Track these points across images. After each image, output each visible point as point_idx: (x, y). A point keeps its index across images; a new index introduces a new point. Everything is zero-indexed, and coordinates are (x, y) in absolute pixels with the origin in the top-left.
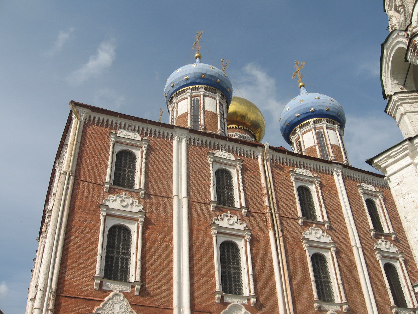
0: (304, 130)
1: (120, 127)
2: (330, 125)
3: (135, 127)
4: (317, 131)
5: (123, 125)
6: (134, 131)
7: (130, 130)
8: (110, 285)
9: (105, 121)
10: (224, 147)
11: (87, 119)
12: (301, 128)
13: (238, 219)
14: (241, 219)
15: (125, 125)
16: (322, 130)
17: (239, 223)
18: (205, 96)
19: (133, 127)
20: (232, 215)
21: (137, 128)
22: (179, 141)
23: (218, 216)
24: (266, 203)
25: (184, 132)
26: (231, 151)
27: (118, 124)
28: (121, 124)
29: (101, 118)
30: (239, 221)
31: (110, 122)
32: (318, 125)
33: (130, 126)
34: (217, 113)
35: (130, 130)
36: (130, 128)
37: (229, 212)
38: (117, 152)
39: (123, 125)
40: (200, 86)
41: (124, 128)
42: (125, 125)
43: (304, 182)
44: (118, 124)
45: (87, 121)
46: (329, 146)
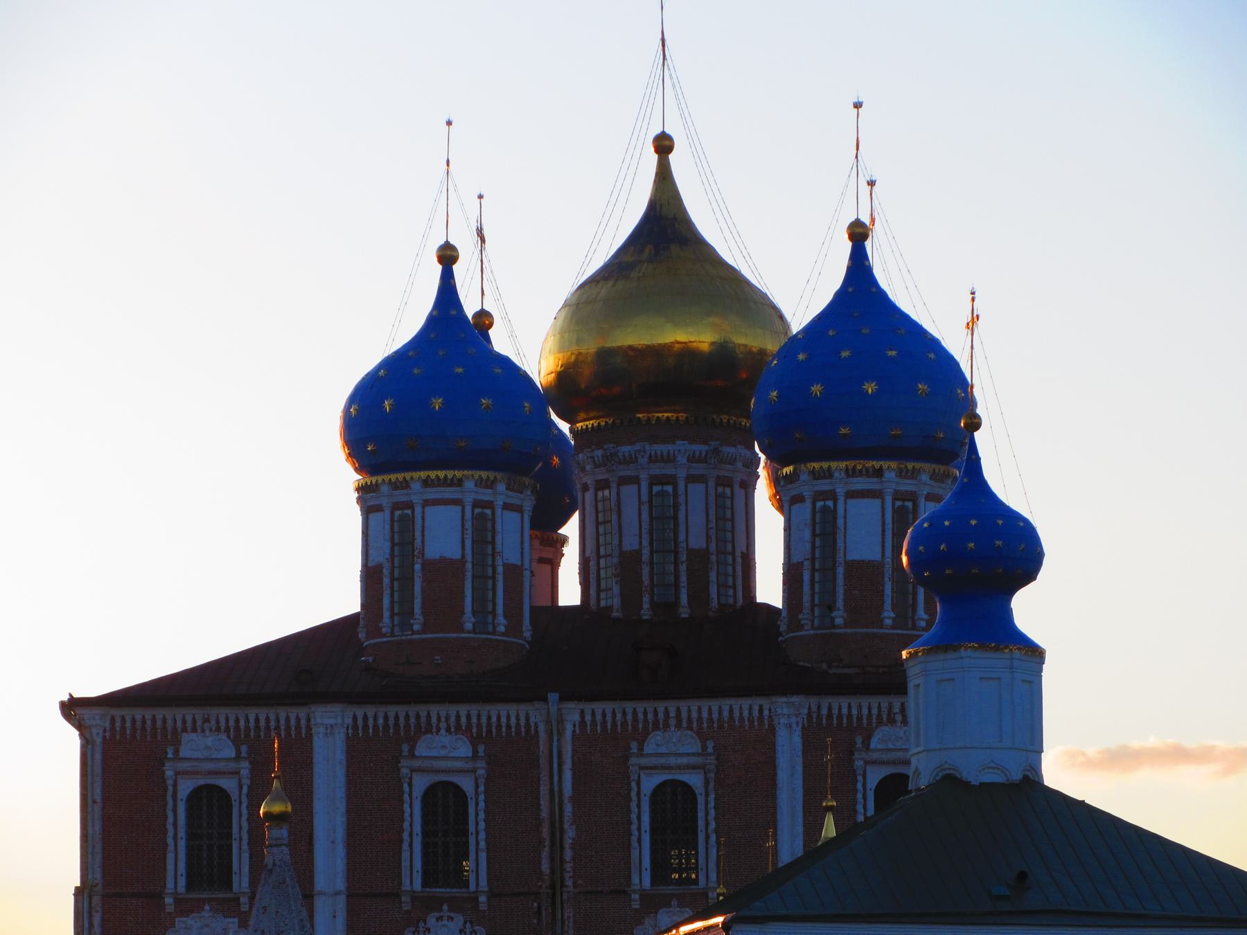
1: (185, 730)
2: (860, 484)
3: (218, 722)
4: (820, 504)
5: (189, 724)
6: (218, 729)
7: (207, 732)
9: (149, 723)
10: (443, 719)
11: (108, 729)
13: (465, 922)
15: (194, 721)
16: (830, 503)
17: (468, 931)
18: (427, 503)
19: (213, 723)
20: (452, 915)
21: (223, 724)
23: (418, 921)
24: (545, 867)
25: (333, 709)
26: (464, 728)
27: (179, 724)
28: (184, 722)
29: (138, 717)
30: (468, 925)
31: (159, 724)
32: (824, 485)
33: (207, 720)
34: (463, 556)
35: (207, 732)
36: (206, 725)
37: (445, 907)
38: (184, 799)
39: (189, 724)
40: (408, 475)
41: (194, 730)
42: (194, 721)
43: (674, 771)
44: (179, 724)
45: (108, 734)
46: (840, 571)
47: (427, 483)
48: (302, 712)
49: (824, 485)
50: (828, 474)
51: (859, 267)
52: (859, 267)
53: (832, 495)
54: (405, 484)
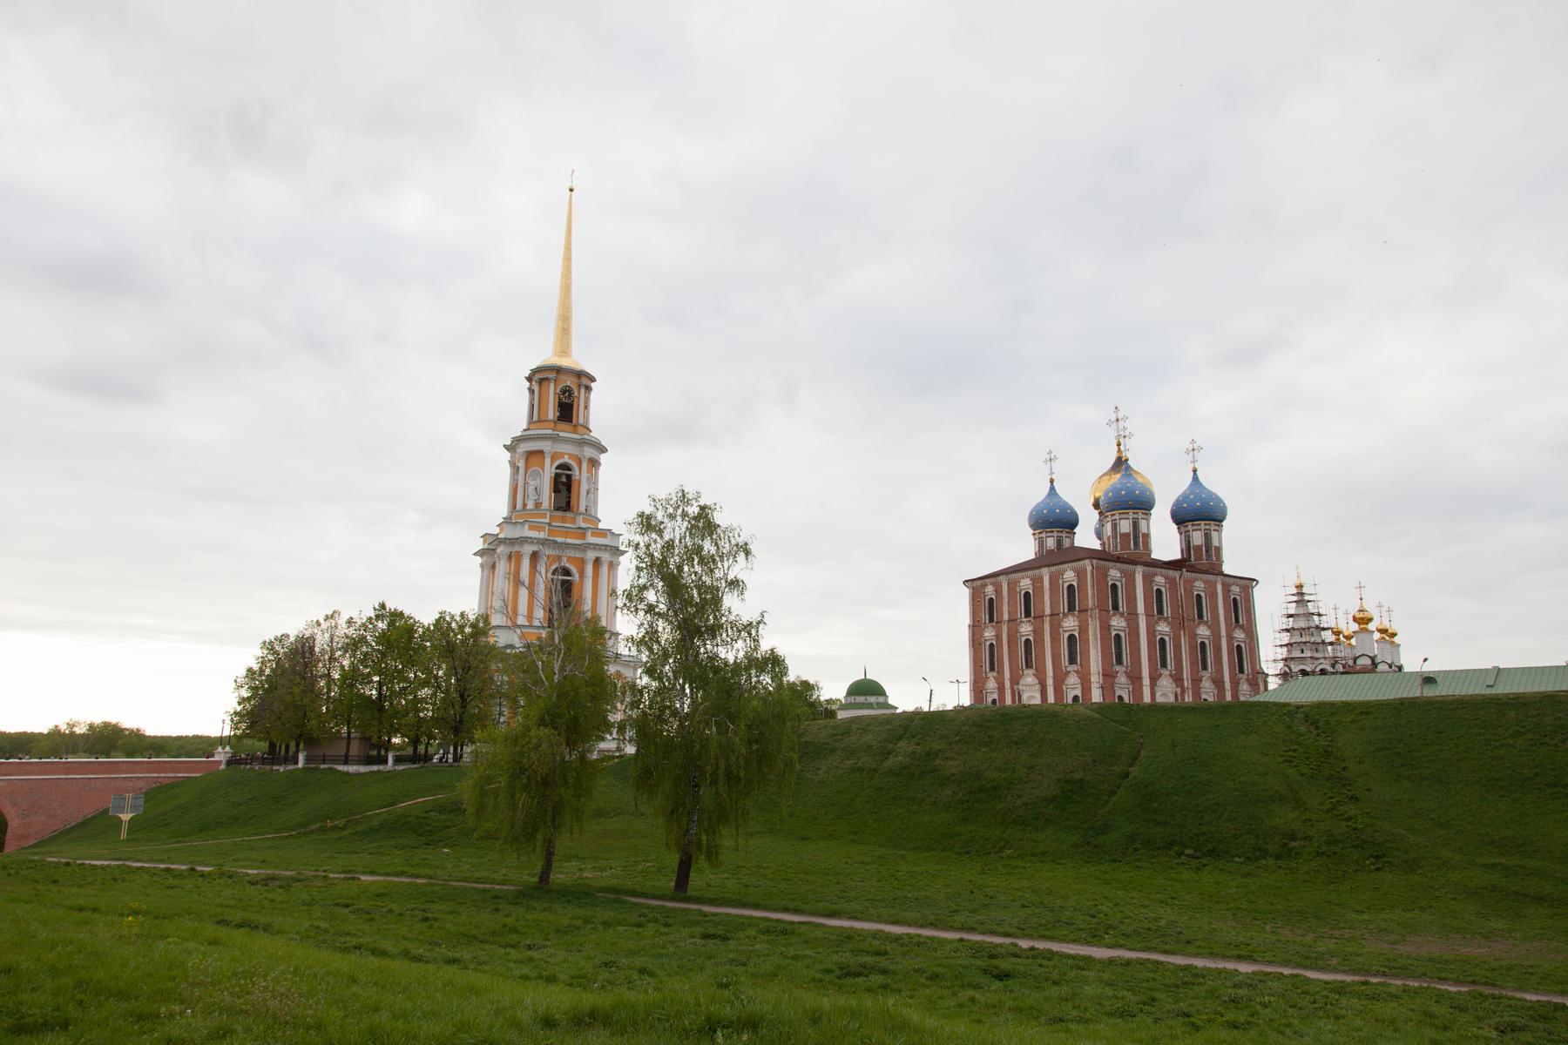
0: (1195, 528)
8: (1118, 668)
12: (1193, 525)
14: (1169, 624)
22: (1139, 573)
32: (1208, 527)
47: (1120, 514)
48: (1134, 567)
49: (1208, 527)
50: (1209, 524)
51: (1195, 478)
52: (1195, 478)
53: (1210, 530)
54: (1137, 513)
